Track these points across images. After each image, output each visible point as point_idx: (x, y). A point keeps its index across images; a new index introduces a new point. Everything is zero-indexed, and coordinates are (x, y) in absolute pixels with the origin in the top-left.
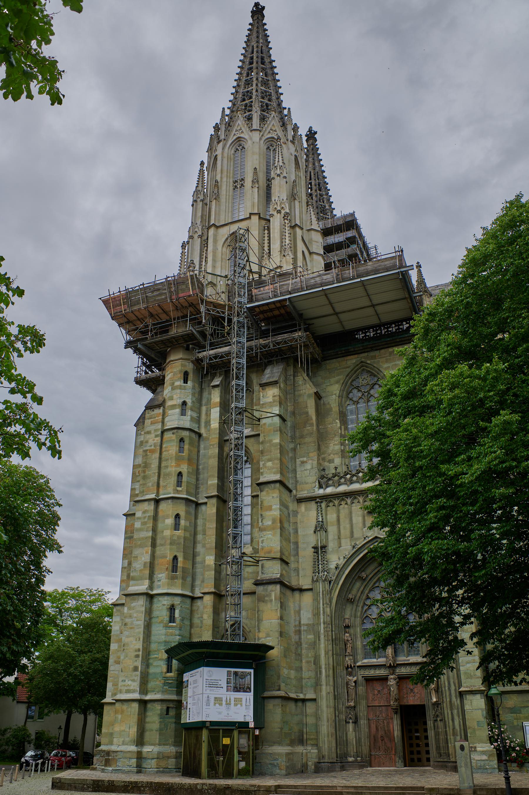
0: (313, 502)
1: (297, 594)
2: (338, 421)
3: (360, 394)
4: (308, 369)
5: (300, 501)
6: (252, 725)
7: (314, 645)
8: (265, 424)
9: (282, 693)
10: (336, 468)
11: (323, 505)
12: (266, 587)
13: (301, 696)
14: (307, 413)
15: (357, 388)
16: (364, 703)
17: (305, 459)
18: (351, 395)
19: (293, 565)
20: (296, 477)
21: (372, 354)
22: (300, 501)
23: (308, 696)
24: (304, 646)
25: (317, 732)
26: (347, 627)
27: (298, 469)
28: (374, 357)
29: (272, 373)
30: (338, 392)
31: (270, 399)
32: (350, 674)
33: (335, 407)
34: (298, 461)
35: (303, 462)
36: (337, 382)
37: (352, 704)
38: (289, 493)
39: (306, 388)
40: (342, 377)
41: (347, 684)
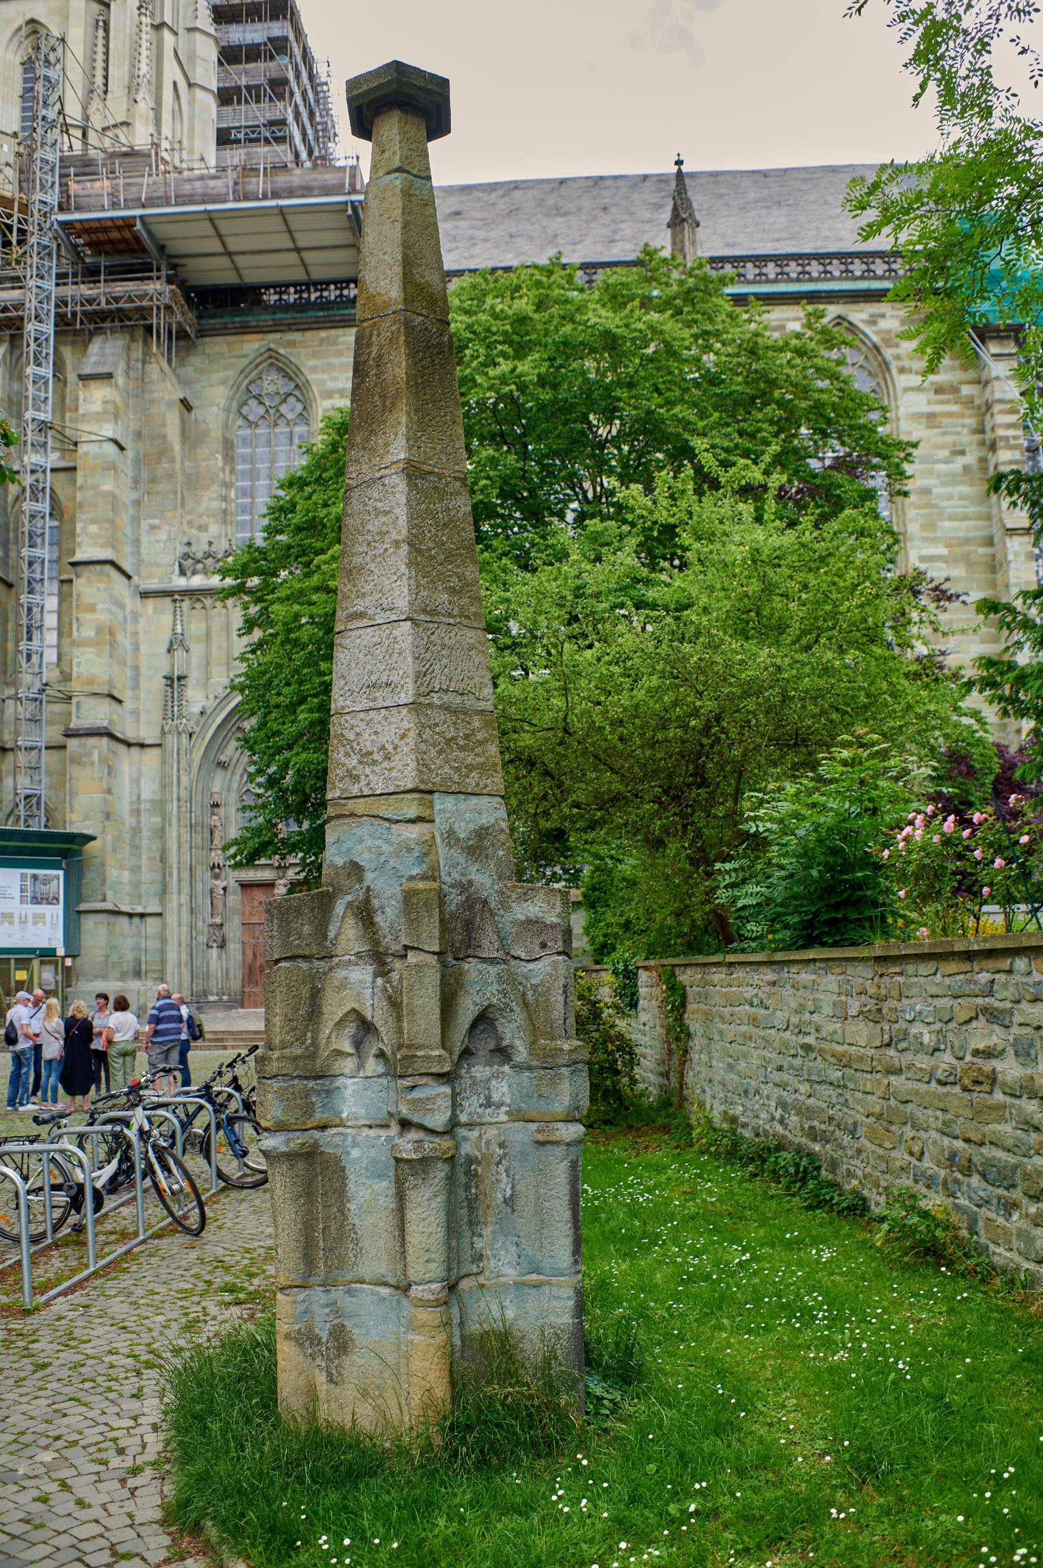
0: (168, 600)
1: (135, 751)
2: (219, 456)
3: (261, 410)
4: (170, 349)
5: (145, 595)
6: (61, 952)
7: (161, 833)
8: (86, 454)
9: (108, 906)
10: (210, 543)
11: (186, 604)
12: (84, 740)
13: (139, 909)
14: (165, 436)
15: (258, 398)
16: (237, 920)
17: (157, 522)
18: (245, 410)
19: (128, 705)
20: (138, 553)
21: (290, 336)
22: (145, 595)
23: (149, 910)
24: (145, 833)
25: (163, 961)
26: (216, 805)
27: (145, 540)
28: (292, 344)
29: (104, 351)
30: (222, 402)
31: (97, 407)
32: (217, 877)
33: (216, 430)
34: (144, 525)
35: (153, 527)
36: (223, 382)
37: (218, 920)
38: (125, 580)
39: (166, 390)
40: (231, 374)
41: (212, 891)
